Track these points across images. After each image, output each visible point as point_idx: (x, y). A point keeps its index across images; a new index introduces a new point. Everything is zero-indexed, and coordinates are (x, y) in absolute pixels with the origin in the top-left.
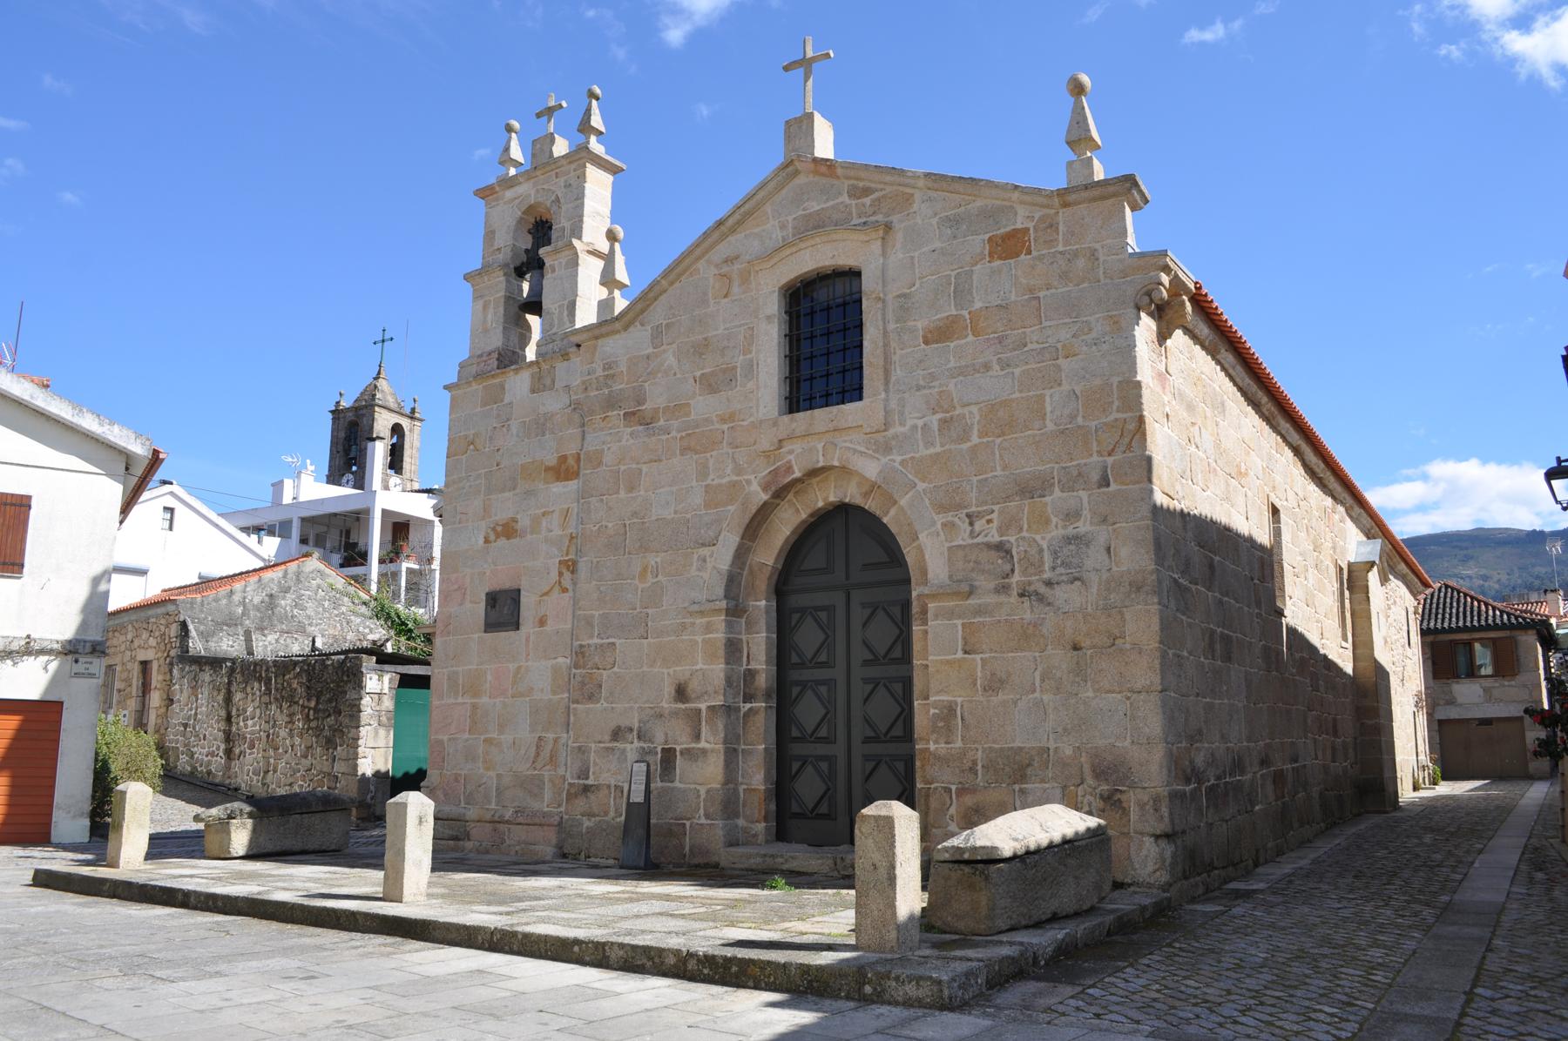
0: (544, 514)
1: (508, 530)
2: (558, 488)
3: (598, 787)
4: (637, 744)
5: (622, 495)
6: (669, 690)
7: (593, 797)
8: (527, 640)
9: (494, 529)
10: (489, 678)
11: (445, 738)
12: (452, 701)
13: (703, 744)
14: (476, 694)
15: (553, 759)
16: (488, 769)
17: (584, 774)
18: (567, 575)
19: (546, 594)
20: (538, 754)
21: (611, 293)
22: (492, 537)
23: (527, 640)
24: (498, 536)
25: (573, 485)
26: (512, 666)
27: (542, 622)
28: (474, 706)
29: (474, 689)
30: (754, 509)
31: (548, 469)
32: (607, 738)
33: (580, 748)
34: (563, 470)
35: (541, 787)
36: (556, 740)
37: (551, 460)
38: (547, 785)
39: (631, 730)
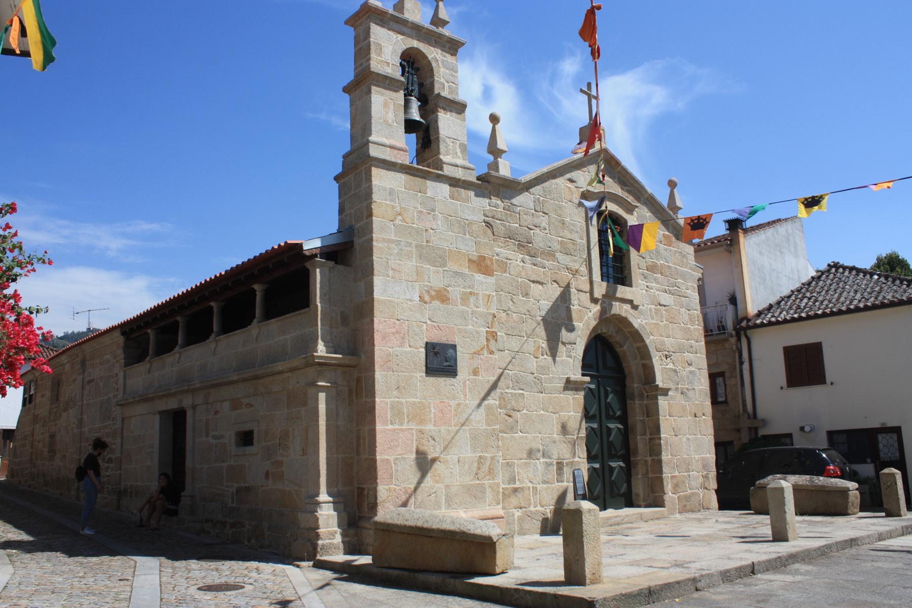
0: (471, 293)
1: (442, 296)
2: (479, 277)
3: (522, 489)
4: (542, 460)
5: (520, 297)
6: (557, 428)
7: (520, 496)
8: (464, 383)
9: (428, 292)
10: (433, 410)
11: (391, 458)
12: (396, 427)
13: (577, 459)
14: (422, 422)
15: (491, 472)
16: (437, 482)
17: (512, 480)
18: (492, 342)
19: (478, 353)
20: (479, 468)
21: (496, 158)
22: (427, 298)
23: (464, 383)
24: (432, 298)
25: (491, 280)
26: (453, 403)
27: (475, 372)
28: (421, 432)
29: (419, 415)
30: (591, 328)
31: (470, 261)
32: (525, 456)
33: (508, 463)
34: (482, 265)
35: (483, 492)
36: (493, 458)
37: (474, 255)
38: (488, 491)
39: (539, 451)
